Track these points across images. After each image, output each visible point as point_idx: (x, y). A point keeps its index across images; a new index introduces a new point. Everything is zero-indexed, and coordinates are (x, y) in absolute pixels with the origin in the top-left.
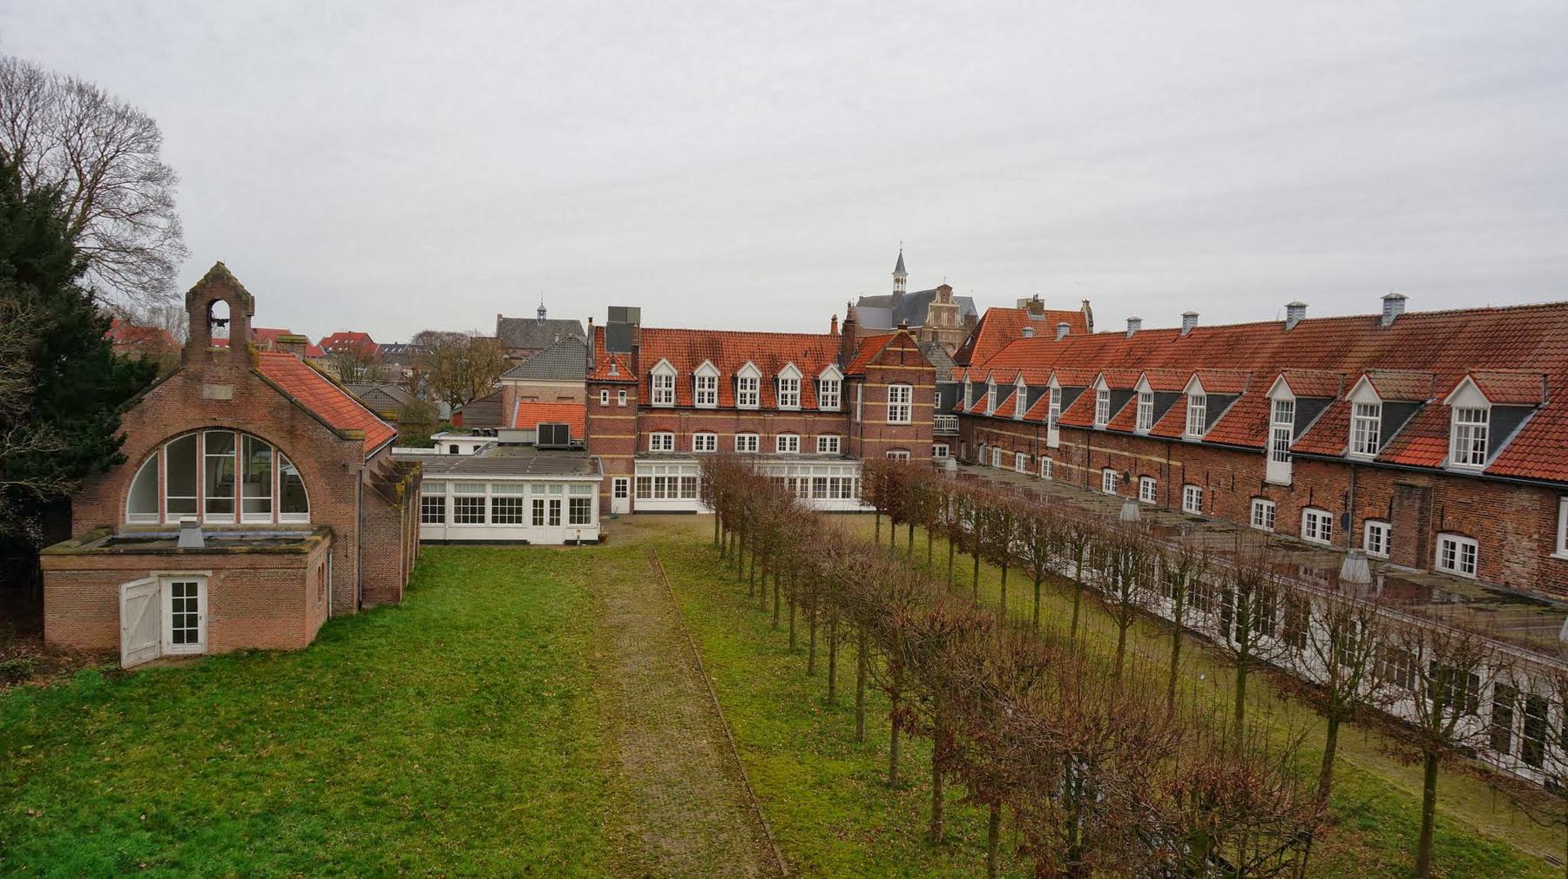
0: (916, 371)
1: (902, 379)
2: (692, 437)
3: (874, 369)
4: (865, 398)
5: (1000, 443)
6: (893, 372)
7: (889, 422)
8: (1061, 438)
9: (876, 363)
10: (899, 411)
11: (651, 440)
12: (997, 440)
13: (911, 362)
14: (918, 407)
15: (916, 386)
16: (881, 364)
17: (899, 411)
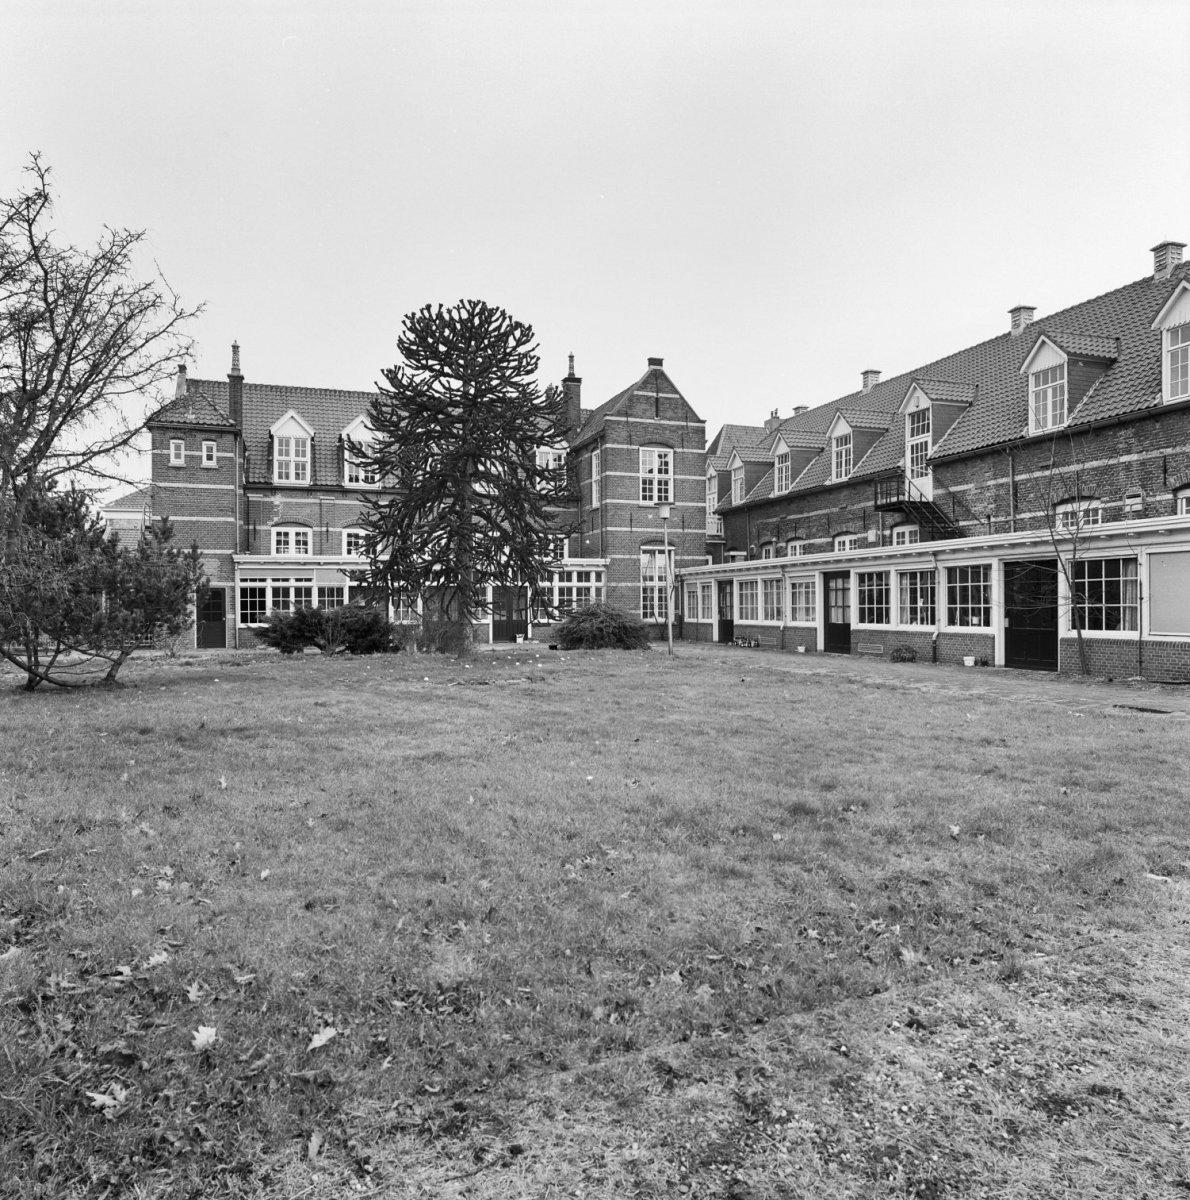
0: (678, 427)
1: (656, 437)
2: (340, 534)
3: (619, 423)
4: (604, 467)
5: (801, 532)
6: (646, 427)
7: (642, 503)
8: (938, 483)
9: (619, 414)
10: (655, 487)
11: (274, 538)
12: (796, 529)
13: (669, 414)
14: (683, 481)
15: (679, 450)
16: (627, 415)
17: (655, 487)
